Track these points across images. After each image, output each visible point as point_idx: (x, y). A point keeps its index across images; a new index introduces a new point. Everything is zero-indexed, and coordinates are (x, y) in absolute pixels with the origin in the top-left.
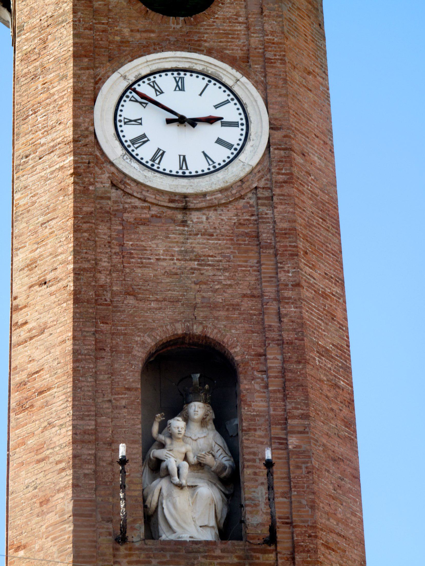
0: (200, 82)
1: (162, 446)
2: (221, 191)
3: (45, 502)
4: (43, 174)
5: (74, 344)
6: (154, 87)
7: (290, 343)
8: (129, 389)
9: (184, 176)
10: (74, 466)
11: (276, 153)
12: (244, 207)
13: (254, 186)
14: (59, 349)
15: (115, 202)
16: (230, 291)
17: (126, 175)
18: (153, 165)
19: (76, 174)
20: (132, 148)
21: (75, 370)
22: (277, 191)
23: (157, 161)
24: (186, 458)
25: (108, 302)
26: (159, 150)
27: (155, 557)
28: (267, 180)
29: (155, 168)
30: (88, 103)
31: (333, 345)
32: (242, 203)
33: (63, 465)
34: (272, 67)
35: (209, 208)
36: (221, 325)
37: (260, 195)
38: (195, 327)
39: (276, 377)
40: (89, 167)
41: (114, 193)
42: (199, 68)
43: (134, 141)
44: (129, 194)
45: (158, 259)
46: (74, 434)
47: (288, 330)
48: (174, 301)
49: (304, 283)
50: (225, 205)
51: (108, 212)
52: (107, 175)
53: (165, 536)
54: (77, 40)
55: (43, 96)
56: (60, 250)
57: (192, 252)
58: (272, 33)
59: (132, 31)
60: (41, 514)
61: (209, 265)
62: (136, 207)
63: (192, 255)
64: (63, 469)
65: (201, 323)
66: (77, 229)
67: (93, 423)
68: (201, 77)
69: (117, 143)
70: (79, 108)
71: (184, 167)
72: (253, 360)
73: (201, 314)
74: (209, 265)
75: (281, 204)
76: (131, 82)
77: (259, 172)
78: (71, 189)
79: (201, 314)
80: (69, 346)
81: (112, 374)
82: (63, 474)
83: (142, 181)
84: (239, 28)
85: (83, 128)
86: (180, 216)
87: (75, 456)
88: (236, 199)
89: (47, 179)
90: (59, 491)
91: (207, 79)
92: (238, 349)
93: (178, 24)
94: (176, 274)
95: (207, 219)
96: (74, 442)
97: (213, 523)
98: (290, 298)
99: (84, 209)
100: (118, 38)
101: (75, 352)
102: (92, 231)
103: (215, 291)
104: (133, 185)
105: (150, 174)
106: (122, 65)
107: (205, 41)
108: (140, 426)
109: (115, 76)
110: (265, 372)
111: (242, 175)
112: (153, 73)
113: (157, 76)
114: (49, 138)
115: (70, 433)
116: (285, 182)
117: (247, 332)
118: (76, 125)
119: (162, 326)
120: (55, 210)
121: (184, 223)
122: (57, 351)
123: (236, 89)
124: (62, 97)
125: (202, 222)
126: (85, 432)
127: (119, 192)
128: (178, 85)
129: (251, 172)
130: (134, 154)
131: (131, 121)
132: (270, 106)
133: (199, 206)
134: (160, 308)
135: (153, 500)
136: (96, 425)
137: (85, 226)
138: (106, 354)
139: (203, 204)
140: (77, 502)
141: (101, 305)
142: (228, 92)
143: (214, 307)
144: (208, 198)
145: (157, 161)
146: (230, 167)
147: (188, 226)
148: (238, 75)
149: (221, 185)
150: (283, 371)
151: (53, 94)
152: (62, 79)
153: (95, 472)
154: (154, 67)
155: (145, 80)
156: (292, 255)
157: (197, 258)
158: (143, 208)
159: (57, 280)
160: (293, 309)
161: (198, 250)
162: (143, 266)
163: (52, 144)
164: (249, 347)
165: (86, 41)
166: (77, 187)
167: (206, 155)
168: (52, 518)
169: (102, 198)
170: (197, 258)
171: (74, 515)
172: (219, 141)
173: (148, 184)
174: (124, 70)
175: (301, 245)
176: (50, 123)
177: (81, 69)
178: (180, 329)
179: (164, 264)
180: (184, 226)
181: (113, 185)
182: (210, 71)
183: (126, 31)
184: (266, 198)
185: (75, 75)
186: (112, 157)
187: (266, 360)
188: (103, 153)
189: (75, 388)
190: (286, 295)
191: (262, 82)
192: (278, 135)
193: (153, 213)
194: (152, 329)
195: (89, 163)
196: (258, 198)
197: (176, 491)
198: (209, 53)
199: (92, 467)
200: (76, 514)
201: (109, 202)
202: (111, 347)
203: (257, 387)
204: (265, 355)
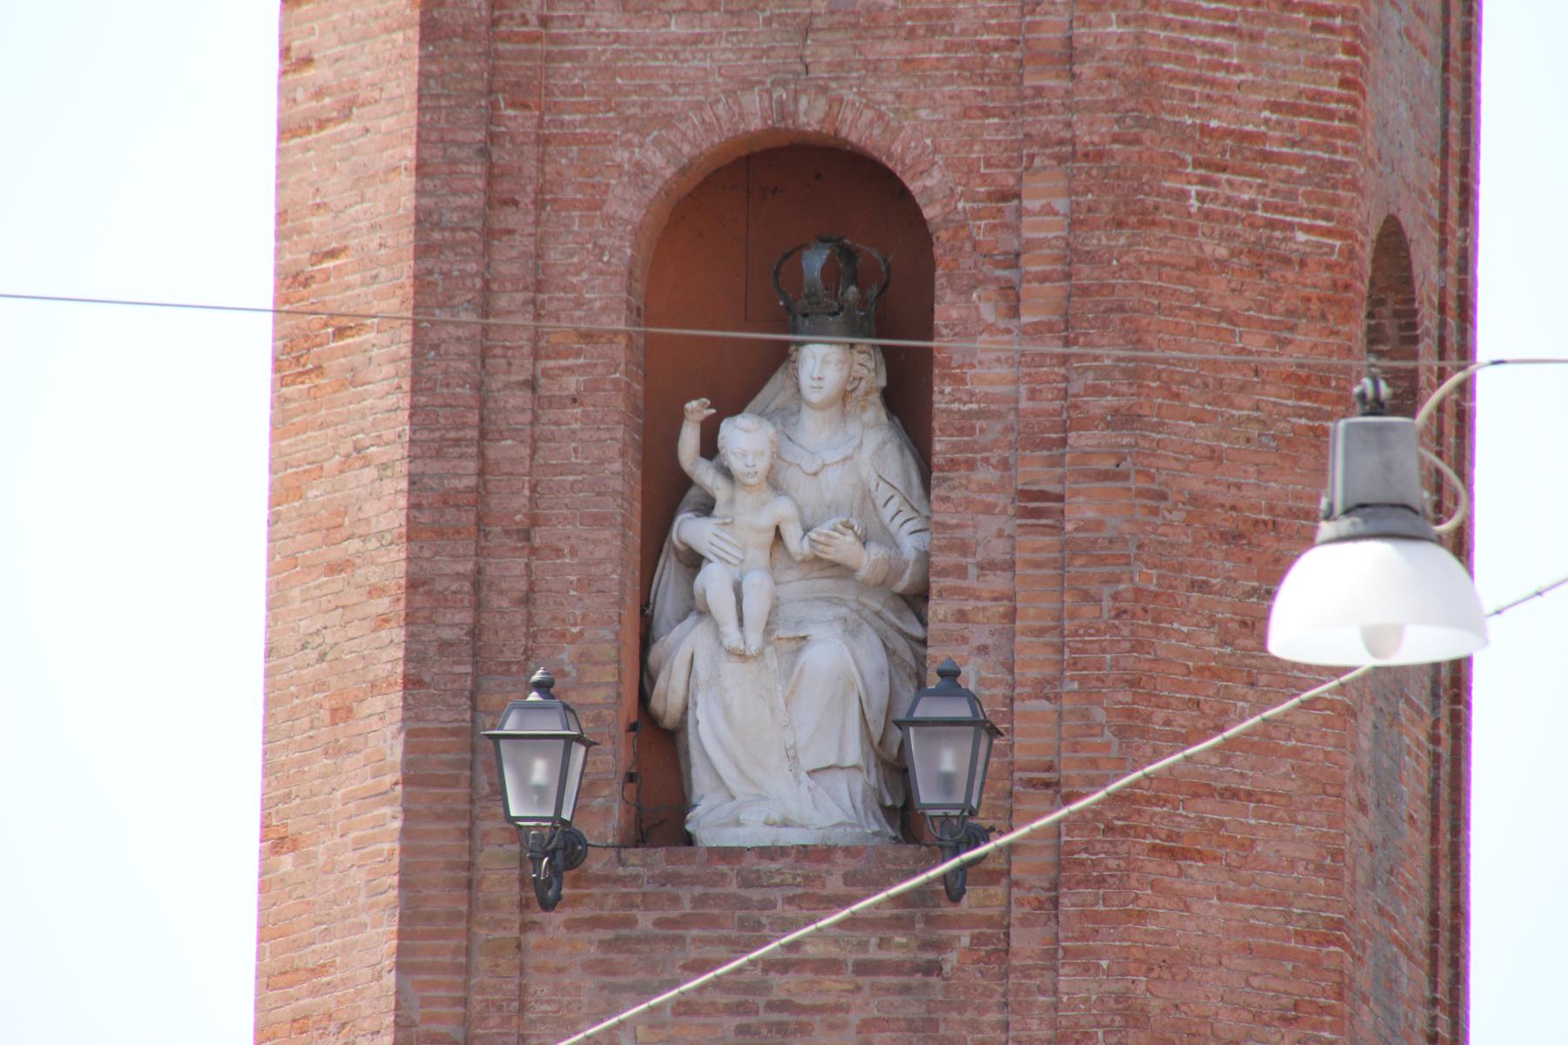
1: (707, 507)
3: (341, 714)
5: (420, 192)
8: (588, 337)
10: (410, 619)
21: (422, 282)
25: (533, 27)
27: (647, 902)
31: (1276, 106)
33: (382, 605)
36: (886, 90)
38: (803, 102)
39: (1044, 278)
46: (414, 507)
47: (1092, 108)
60: (335, 750)
64: (384, 620)
65: (823, 90)
67: (472, 466)
72: (977, 215)
73: (823, 53)
79: (823, 53)
81: (539, 286)
82: (384, 634)
92: (933, 180)
96: (413, 532)
97: (854, 753)
101: (424, 220)
108: (617, 466)
115: (402, 502)
117: (966, 113)
119: (699, 106)
126: (447, 500)
134: (698, 39)
135: (669, 694)
136: (481, 473)
140: (415, 736)
141: (508, 38)
150: (1072, 255)
153: (475, 632)
160: (1114, 28)
164: (971, 169)
171: (407, 781)
187: (1020, 212)
189: (419, 345)
194: (668, 121)
197: (731, 668)
199: (465, 617)
200: (412, 778)
202: (540, 191)
203: (988, 313)
204: (1018, 196)
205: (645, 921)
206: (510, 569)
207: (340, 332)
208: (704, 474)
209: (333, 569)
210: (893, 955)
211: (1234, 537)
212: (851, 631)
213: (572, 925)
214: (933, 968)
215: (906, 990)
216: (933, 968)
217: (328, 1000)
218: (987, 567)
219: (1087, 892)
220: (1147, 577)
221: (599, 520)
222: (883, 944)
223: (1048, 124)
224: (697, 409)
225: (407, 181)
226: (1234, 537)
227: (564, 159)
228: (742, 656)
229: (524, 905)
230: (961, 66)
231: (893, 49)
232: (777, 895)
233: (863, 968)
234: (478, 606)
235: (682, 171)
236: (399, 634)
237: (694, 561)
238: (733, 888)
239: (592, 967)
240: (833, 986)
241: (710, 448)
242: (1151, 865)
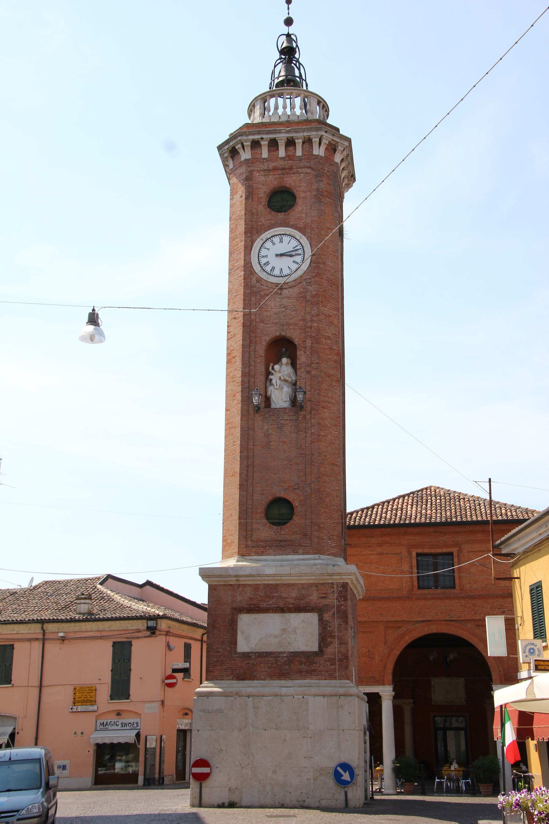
0: (288, 238)
1: (273, 374)
2: (294, 281)
3: (234, 396)
4: (235, 277)
5: (243, 342)
6: (272, 242)
7: (314, 337)
8: (260, 356)
9: (281, 276)
10: (242, 385)
11: (313, 265)
12: (302, 286)
13: (305, 278)
14: (238, 343)
15: (258, 288)
16: (295, 318)
17: (261, 278)
18: (271, 273)
19: (244, 279)
20: (264, 267)
21: (243, 351)
22: (313, 280)
23: (272, 271)
24: (280, 378)
25: (254, 326)
26: (273, 267)
28: (310, 275)
29: (271, 274)
30: (249, 251)
31: (332, 334)
32: (301, 284)
33: (239, 384)
34: (314, 231)
35: (289, 288)
36: (292, 331)
37: (307, 282)
39: (309, 349)
40: (249, 276)
41: (258, 285)
42: (288, 233)
43: (264, 264)
44: (262, 285)
45: (271, 308)
46: (242, 374)
47: (313, 332)
48: (276, 324)
49: (321, 314)
50: (295, 286)
51: (255, 292)
52: (255, 278)
53: (273, 406)
54: (246, 226)
55: (236, 247)
56: (240, 307)
57: (283, 305)
58: (314, 217)
59: (265, 220)
60: (233, 400)
61: (289, 309)
62: (264, 289)
63: (283, 306)
64: (239, 386)
65: (285, 331)
66: (244, 300)
67: (248, 369)
68: (289, 236)
69: (259, 265)
70: (246, 253)
71: (281, 273)
72: (301, 343)
73: (285, 328)
74: (289, 309)
75: (314, 284)
76: (264, 241)
77: (307, 272)
78: (243, 284)
79: (285, 328)
80: (241, 342)
81: (255, 351)
82: (239, 387)
83: (266, 280)
84: (303, 215)
85: (247, 261)
86: (279, 292)
87: (242, 381)
88: (299, 284)
89: (237, 280)
90: (238, 393)
91: (291, 237)
92: (297, 340)
93: (282, 216)
94: (277, 313)
95: (289, 292)
96: (242, 376)
97: (288, 400)
98: (315, 320)
99: (247, 292)
100: (260, 224)
101: (243, 345)
102: (250, 300)
103: (290, 319)
104: (264, 281)
105: (269, 277)
106: (261, 235)
107: (291, 222)
108: (263, 369)
109: (259, 239)
110: (305, 348)
111: (301, 274)
112: (272, 237)
113: (273, 238)
114: (238, 264)
115: (241, 373)
116: (316, 276)
117: (300, 333)
118: (245, 260)
119: (272, 333)
120: (238, 292)
121: (281, 294)
122: (238, 344)
123: (301, 240)
124: (241, 248)
125: (287, 293)
126: (246, 373)
127: (259, 284)
128: (280, 241)
129: (304, 273)
130: (264, 269)
131: (264, 256)
132: (312, 246)
133: (286, 287)
134: (272, 327)
135: (269, 393)
136: (249, 370)
137: (247, 298)
138: (253, 345)
139: (287, 287)
140: (242, 397)
141: (252, 327)
142: (298, 242)
143: (290, 324)
144: (289, 284)
145: (272, 271)
146: (297, 271)
147: (282, 295)
148: (301, 235)
149: (294, 279)
150: (312, 347)
151: (239, 247)
152: (241, 241)
153: (249, 386)
154: (272, 234)
155: (269, 240)
156: (316, 304)
157: (285, 307)
158: (267, 289)
159: (238, 318)
161: (285, 304)
162: (266, 311)
163: (238, 266)
165: (249, 226)
166: (245, 284)
167: (289, 268)
168: (236, 402)
169: (253, 287)
170: (285, 307)
171: (241, 401)
172: (294, 262)
173: (269, 280)
174: (261, 237)
175: (320, 299)
176: (238, 258)
177: (247, 238)
178: (278, 334)
179: (273, 310)
180: (281, 295)
181: (257, 281)
182: (292, 234)
183: (263, 221)
184: (309, 283)
185: (245, 240)
186: (257, 271)
187: (306, 343)
188: (254, 270)
189: (243, 357)
190: (313, 319)
191: (310, 237)
192: (314, 257)
193: (271, 291)
194: (268, 335)
195: (249, 274)
196: (307, 283)
197: (275, 390)
198: (292, 227)
199: (247, 385)
200: (242, 401)
201: (256, 288)
202: (255, 342)
203: (303, 353)
204: (306, 341)
205: (267, 416)
206: (252, 380)
207: (234, 358)
208: (272, 371)
209: (233, 382)
210: (294, 418)
211: (329, 376)
212: (288, 387)
213: (259, 416)
214: (298, 420)
215: (295, 422)
216: (298, 420)
217: (233, 425)
218: (303, 379)
219: (314, 411)
220: (320, 379)
221: (261, 375)
222: (292, 417)
223: (309, 334)
224: (271, 364)
225: (241, 341)
226: (329, 376)
227: (258, 339)
228: (277, 389)
229: (254, 414)
230: (299, 329)
231: (292, 327)
232: (281, 413)
233: (290, 420)
234: (249, 383)
235: (270, 340)
236: (241, 387)
237: (271, 380)
238: (276, 412)
239: (261, 420)
240: (287, 422)
241: (273, 369)
242: (321, 409)
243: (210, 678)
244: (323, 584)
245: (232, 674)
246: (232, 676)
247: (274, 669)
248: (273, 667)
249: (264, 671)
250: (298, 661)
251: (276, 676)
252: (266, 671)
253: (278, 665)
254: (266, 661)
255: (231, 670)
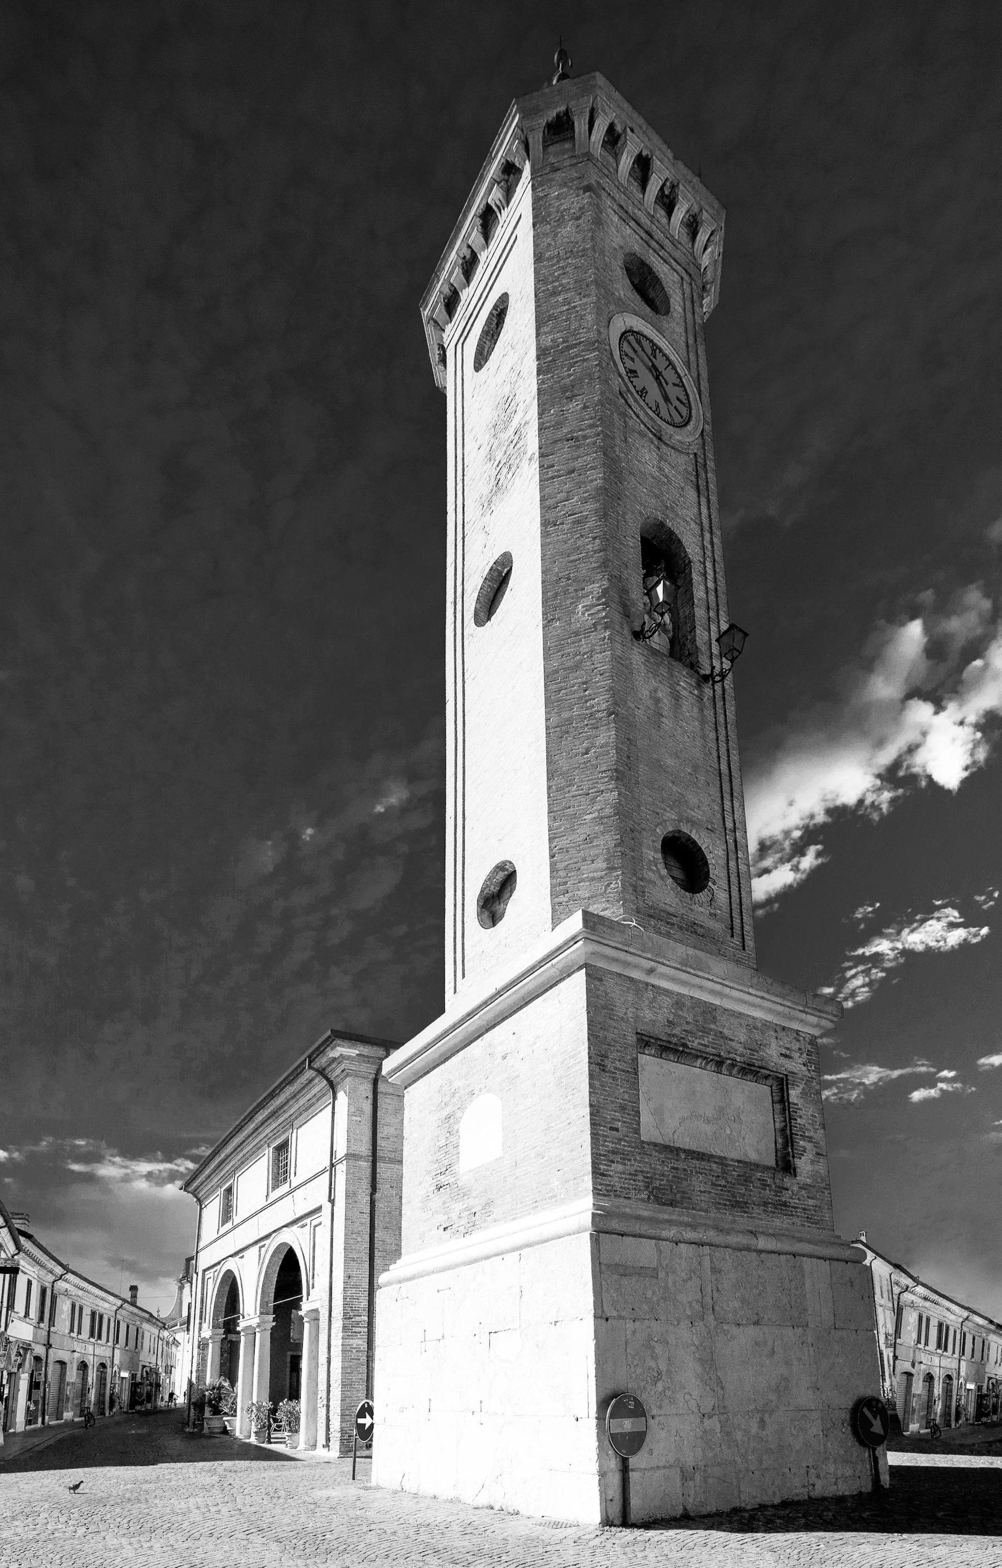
243: (601, 1190)
244: (784, 1028)
245: (647, 1187)
246: (646, 1192)
247: (721, 1190)
248: (720, 1185)
249: (704, 1192)
250: (759, 1180)
251: (725, 1205)
252: (710, 1192)
253: (728, 1182)
254: (705, 1169)
255: (644, 1177)
